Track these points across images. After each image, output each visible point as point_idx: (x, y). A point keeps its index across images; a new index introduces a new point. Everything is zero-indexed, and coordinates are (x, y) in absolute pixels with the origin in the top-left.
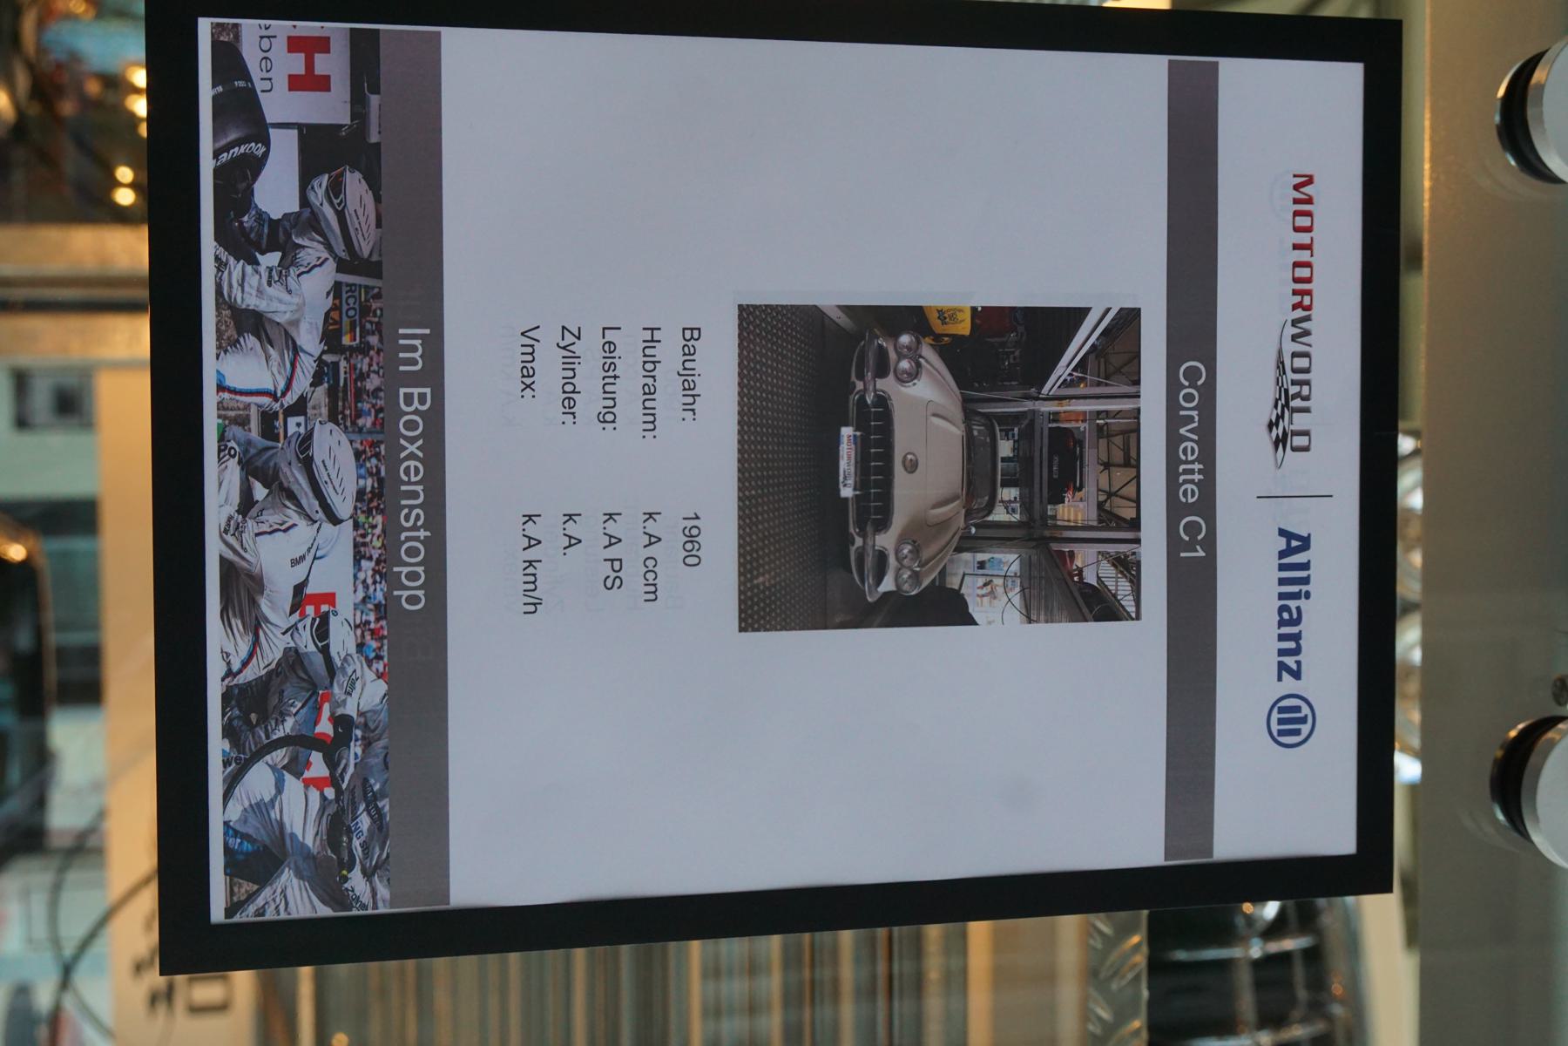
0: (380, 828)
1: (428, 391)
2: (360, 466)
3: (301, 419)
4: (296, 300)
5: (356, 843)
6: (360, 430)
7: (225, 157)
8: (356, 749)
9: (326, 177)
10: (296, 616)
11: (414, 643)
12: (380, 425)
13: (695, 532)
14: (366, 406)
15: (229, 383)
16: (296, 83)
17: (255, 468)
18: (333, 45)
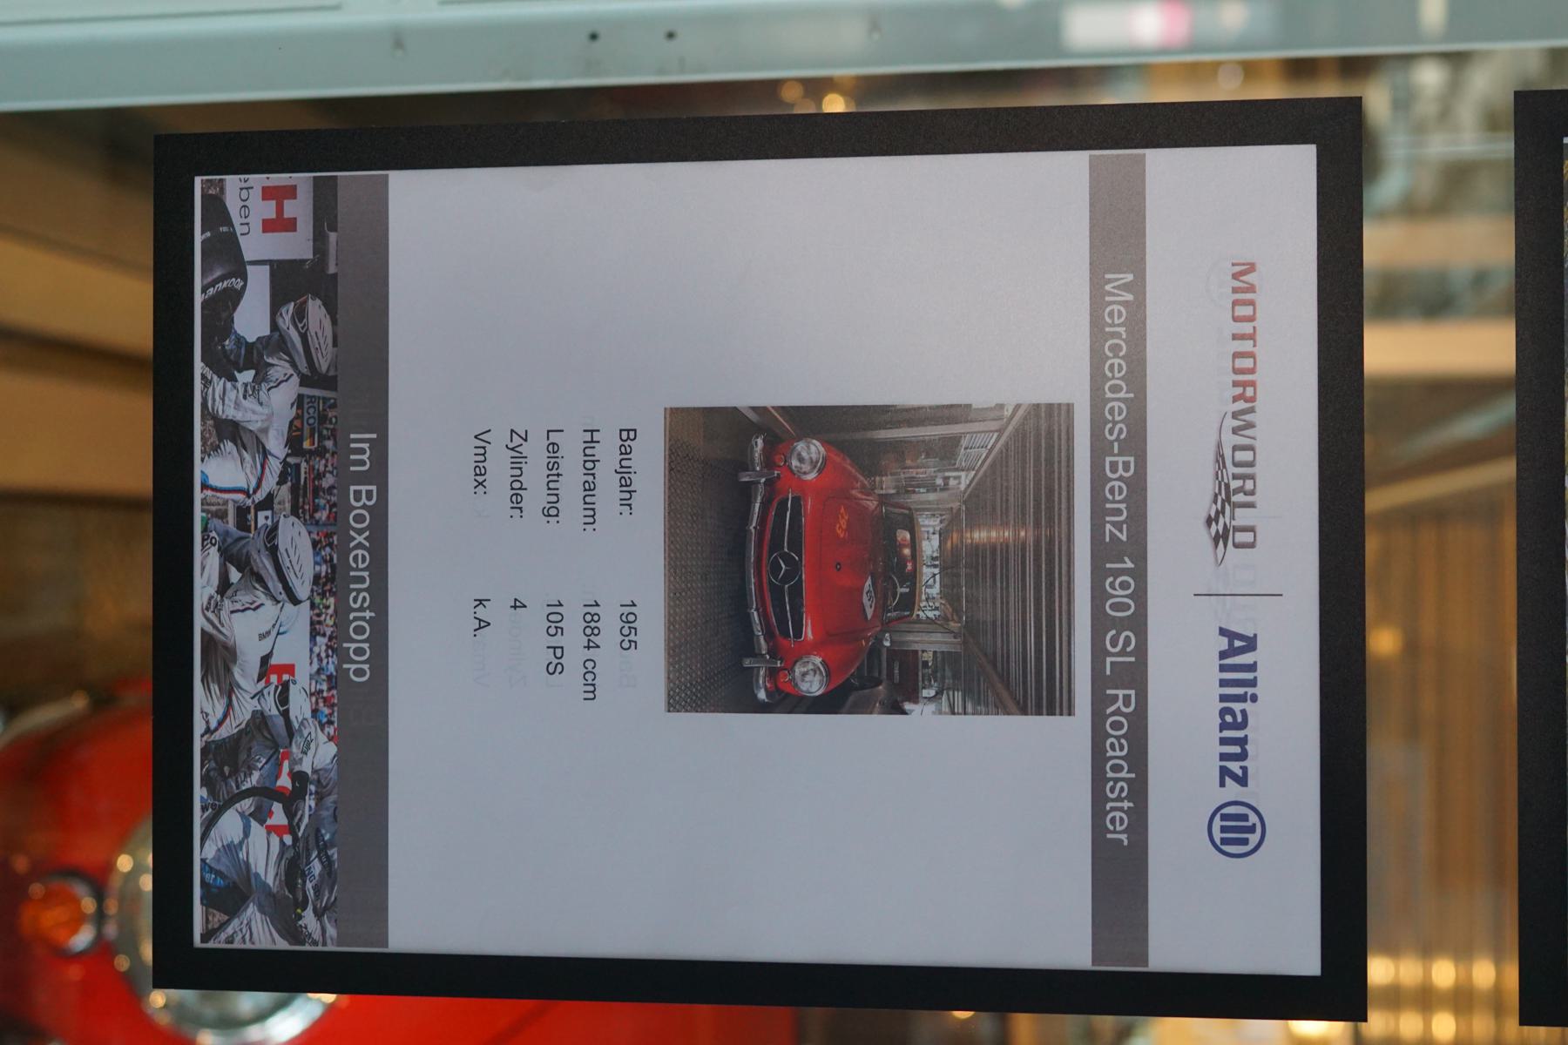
0: (329, 874)
1: (374, 488)
2: (316, 553)
3: (268, 513)
4: (266, 411)
5: (309, 885)
6: (317, 523)
7: (211, 291)
8: (310, 802)
9: (291, 306)
10: (263, 683)
11: (360, 709)
12: (333, 519)
13: (631, 618)
14: (322, 502)
15: (212, 482)
16: (269, 226)
17: (231, 556)
18: (299, 191)
